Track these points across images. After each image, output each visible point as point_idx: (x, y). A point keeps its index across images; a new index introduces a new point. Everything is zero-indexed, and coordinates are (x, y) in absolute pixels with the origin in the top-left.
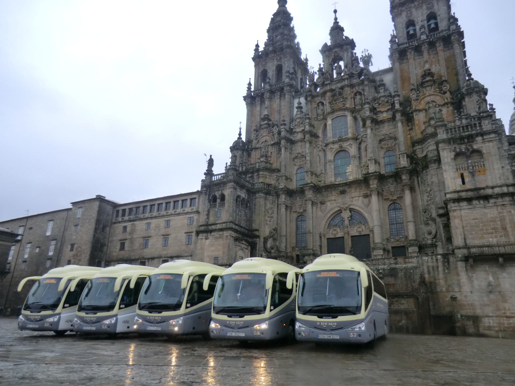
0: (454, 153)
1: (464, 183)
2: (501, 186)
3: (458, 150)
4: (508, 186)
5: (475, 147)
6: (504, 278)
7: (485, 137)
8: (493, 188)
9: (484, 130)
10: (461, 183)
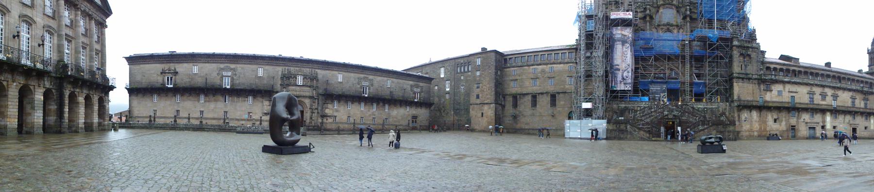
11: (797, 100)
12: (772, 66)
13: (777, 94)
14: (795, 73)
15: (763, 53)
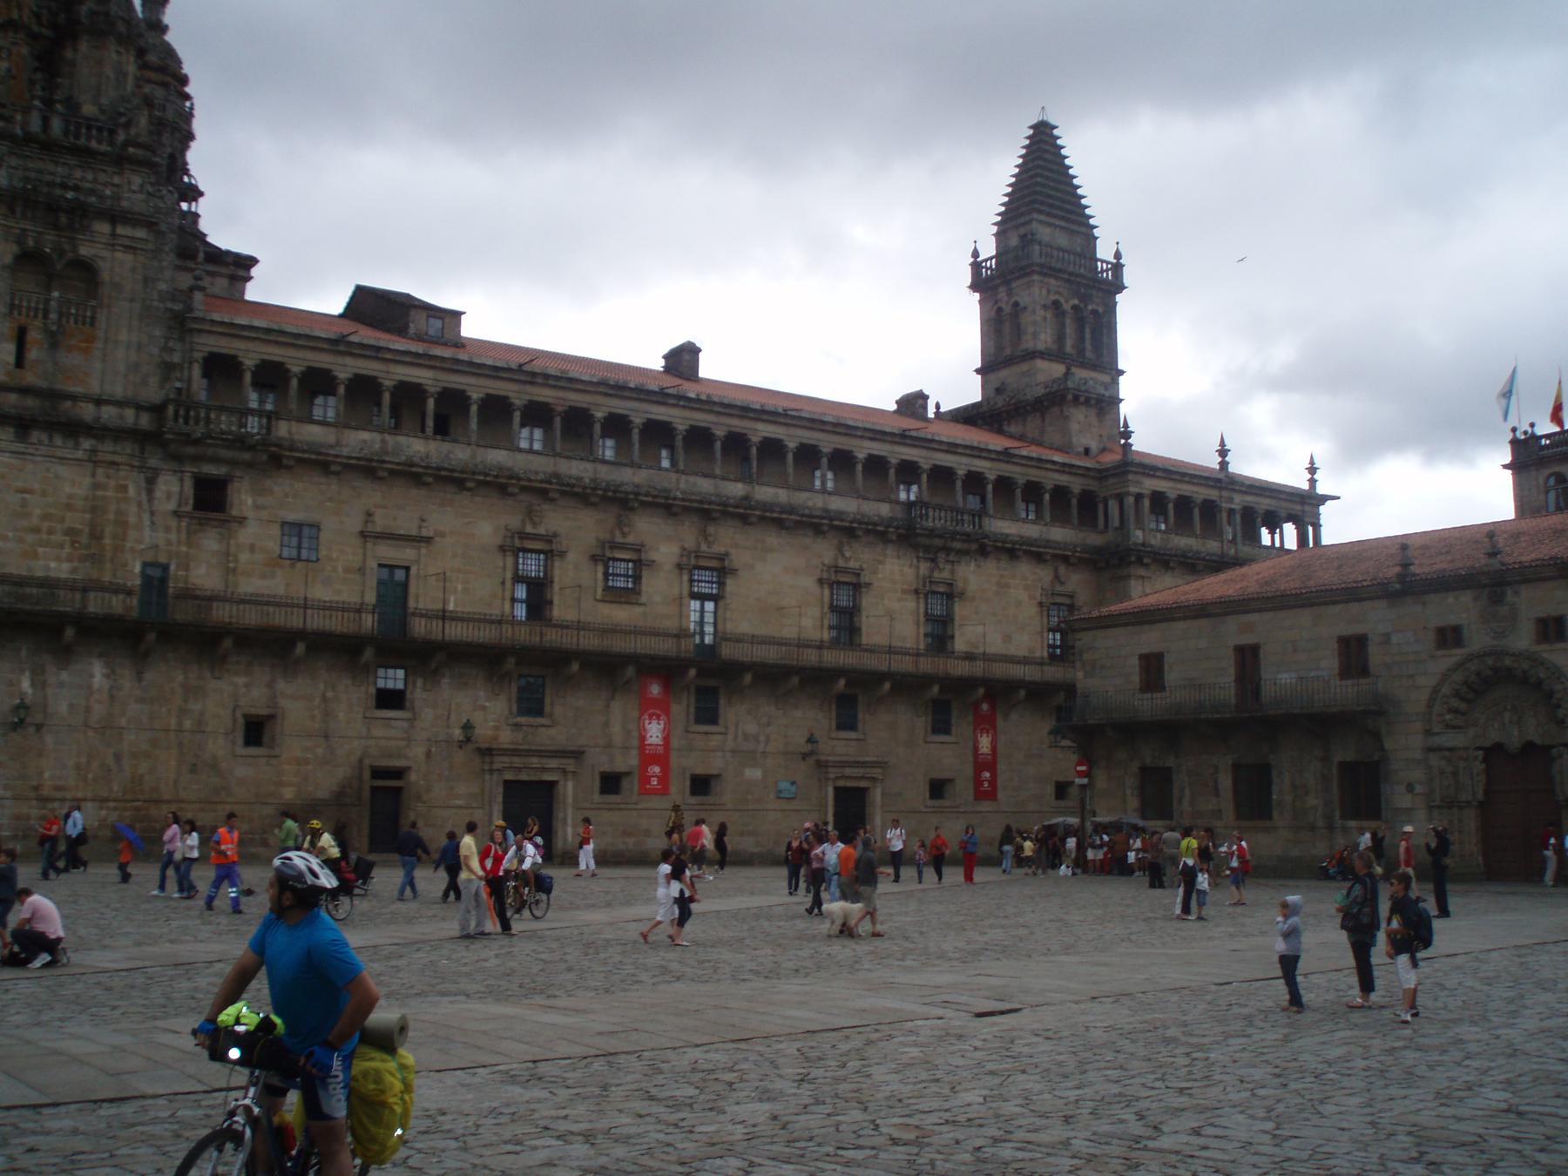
0: (15, 248)
1: (20, 362)
2: (120, 404)
3: (31, 243)
4: (139, 408)
5: (84, 251)
6: (61, 685)
7: (120, 230)
8: (99, 402)
9: (125, 204)
10: (11, 359)
11: (423, 596)
12: (251, 355)
13: (294, 548)
14: (448, 414)
15: (241, 266)
